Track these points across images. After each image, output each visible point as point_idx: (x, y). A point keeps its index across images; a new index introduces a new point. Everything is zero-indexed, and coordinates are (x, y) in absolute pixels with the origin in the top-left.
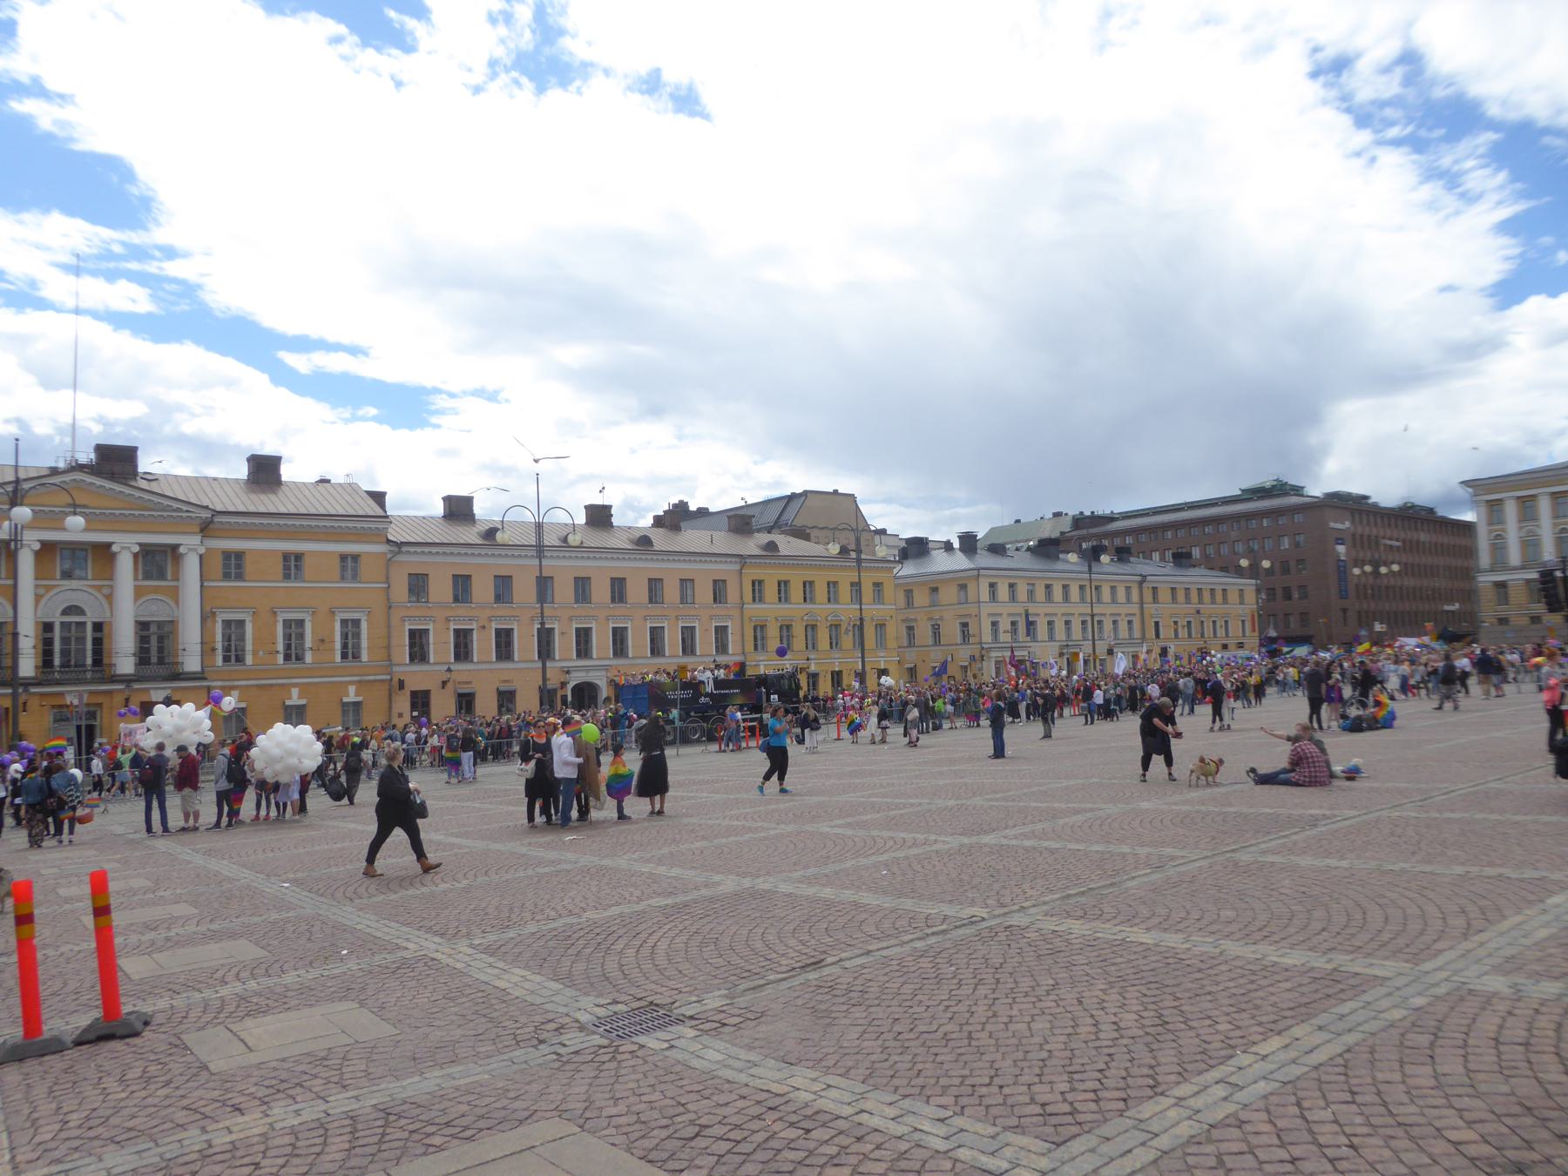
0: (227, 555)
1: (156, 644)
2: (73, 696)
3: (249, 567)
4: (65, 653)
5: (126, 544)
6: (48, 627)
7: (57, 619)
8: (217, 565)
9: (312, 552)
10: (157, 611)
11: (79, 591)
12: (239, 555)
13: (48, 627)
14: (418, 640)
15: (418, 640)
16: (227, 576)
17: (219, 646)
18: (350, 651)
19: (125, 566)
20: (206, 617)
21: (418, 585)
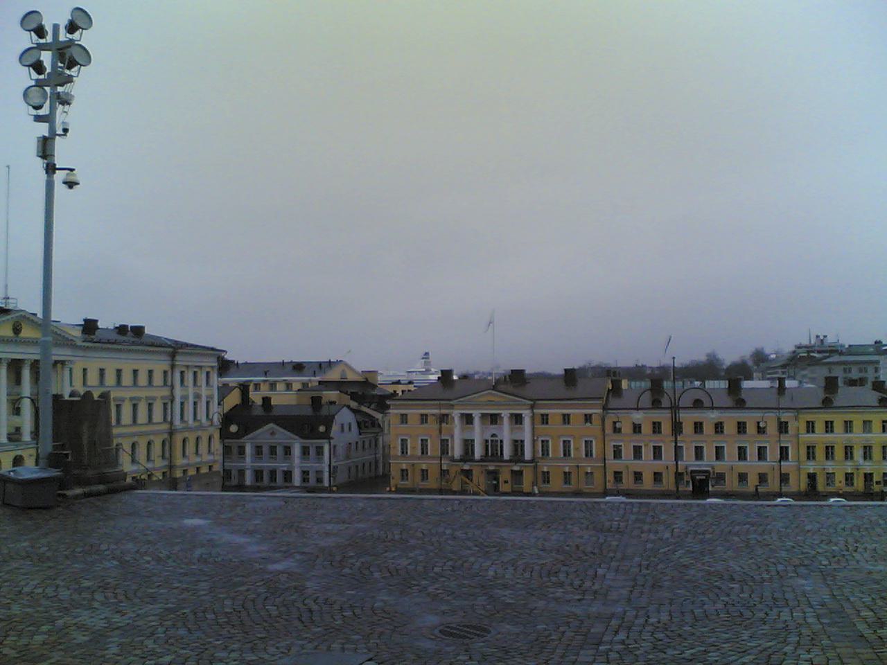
0: (542, 415)
1: (518, 445)
5: (505, 414)
6: (487, 441)
7: (490, 439)
8: (538, 419)
9: (573, 414)
10: (518, 437)
11: (493, 429)
18: (589, 453)
19: (506, 420)
20: (534, 442)
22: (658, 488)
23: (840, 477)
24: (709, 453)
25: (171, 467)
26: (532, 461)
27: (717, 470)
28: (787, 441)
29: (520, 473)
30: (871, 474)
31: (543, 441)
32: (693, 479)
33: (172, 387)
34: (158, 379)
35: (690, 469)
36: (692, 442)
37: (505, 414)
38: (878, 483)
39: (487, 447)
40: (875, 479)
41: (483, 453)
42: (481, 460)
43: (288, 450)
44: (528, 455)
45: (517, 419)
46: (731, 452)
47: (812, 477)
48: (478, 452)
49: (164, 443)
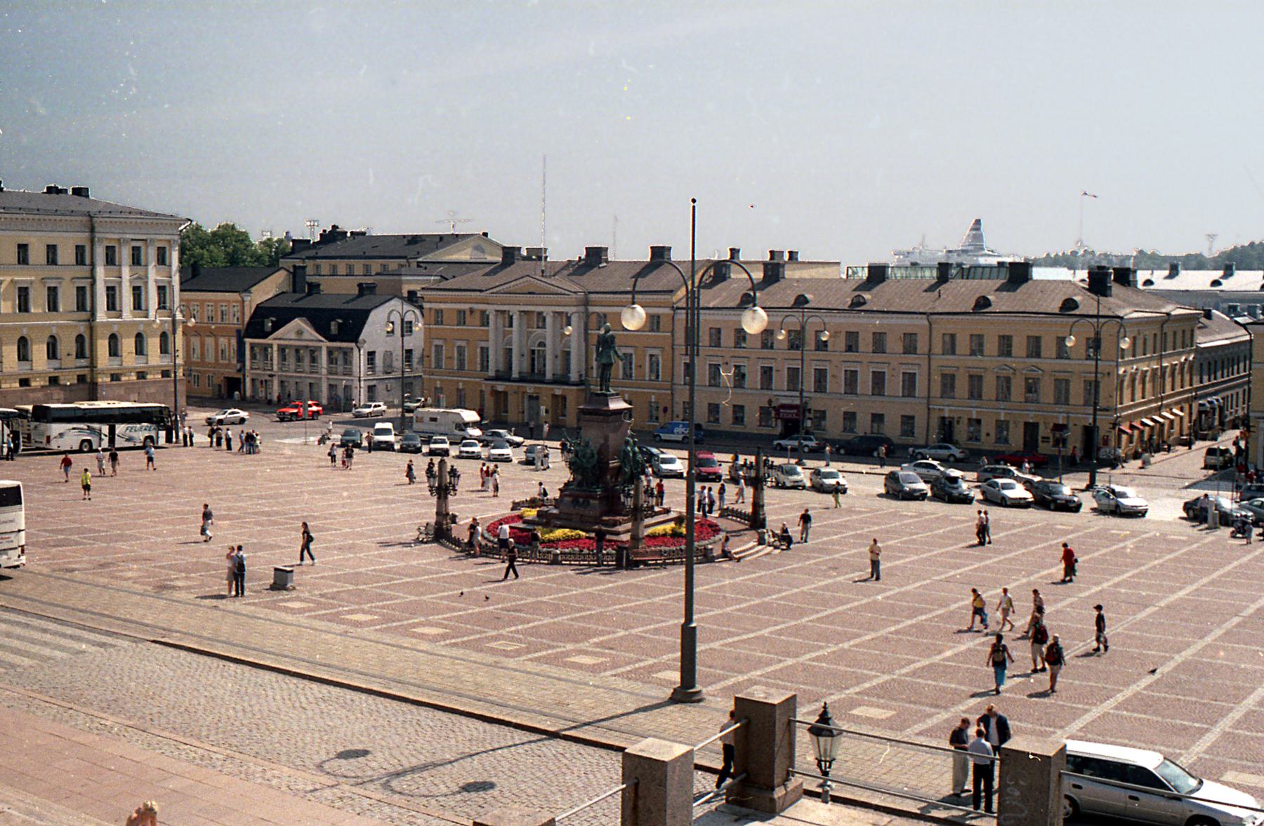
2: (530, 388)
5: (547, 311)
6: (533, 352)
19: (549, 320)
22: (738, 429)
23: (988, 427)
25: (92, 366)
26: (581, 383)
29: (564, 398)
33: (93, 265)
34: (66, 255)
38: (1045, 439)
39: (533, 359)
41: (526, 366)
42: (522, 379)
43: (313, 354)
49: (80, 339)
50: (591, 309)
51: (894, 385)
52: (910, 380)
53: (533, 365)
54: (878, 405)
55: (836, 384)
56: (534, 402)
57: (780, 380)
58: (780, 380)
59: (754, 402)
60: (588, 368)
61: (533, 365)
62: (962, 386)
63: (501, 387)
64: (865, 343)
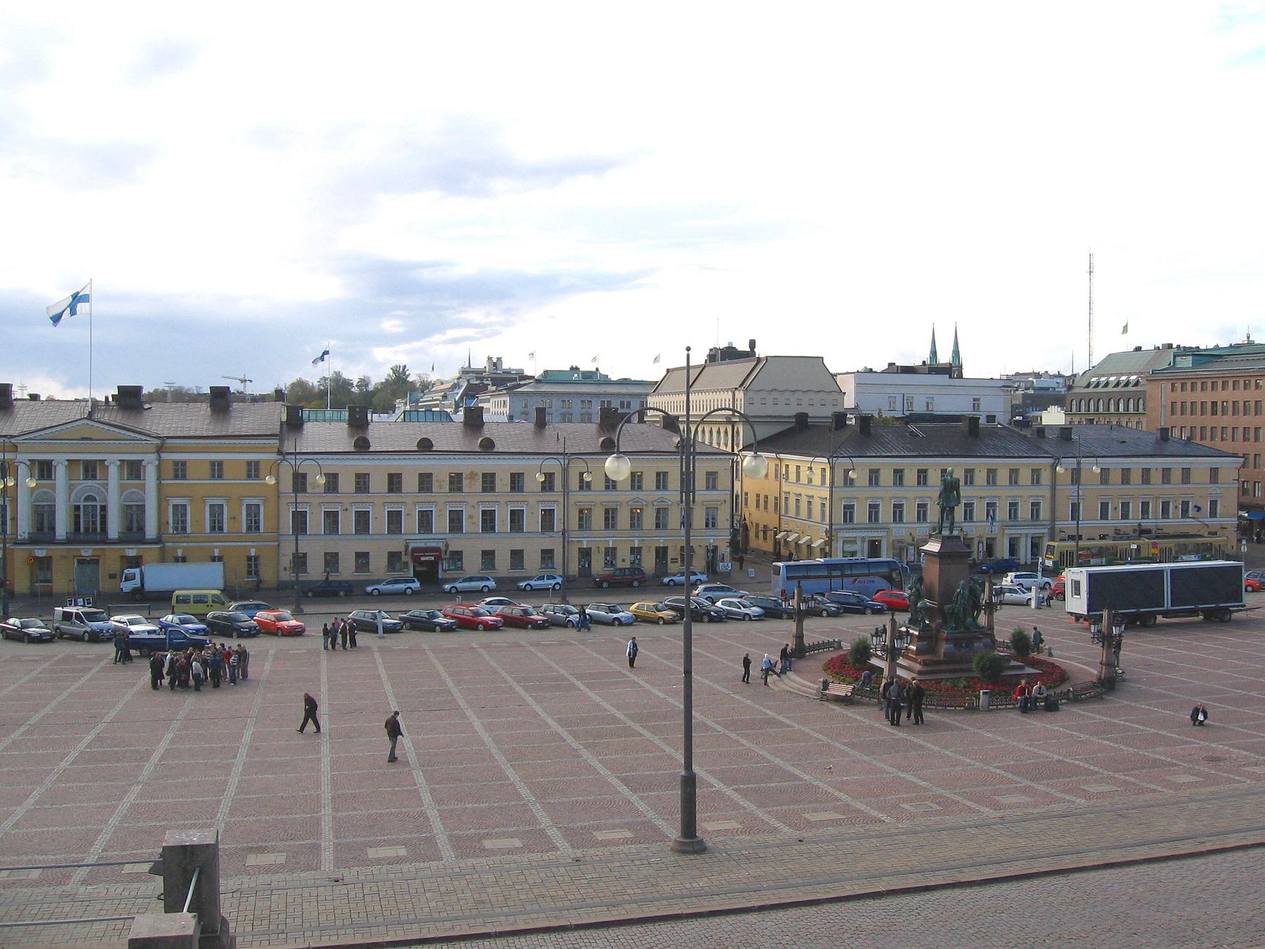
0: (176, 463)
1: (133, 517)
2: (87, 551)
3: (190, 471)
4: (87, 522)
5: (113, 459)
6: (77, 508)
7: (82, 504)
8: (170, 470)
12: (184, 463)
13: (77, 508)
14: (300, 521)
15: (300, 521)
16: (176, 477)
17: (171, 521)
18: (253, 525)
19: (113, 471)
21: (300, 482)
24: (441, 523)
26: (158, 541)
27: (454, 547)
28: (554, 500)
30: (665, 549)
31: (175, 507)
32: (416, 560)
35: (412, 545)
36: (415, 504)
37: (113, 459)
38: (674, 560)
39: (77, 517)
40: (671, 554)
42: (68, 541)
44: (151, 531)
45: (134, 469)
46: (472, 522)
47: (585, 554)
48: (62, 527)
50: (165, 456)
51: (532, 521)
52: (548, 515)
53: (77, 523)
54: (488, 542)
55: (472, 522)
56: (88, 569)
57: (410, 523)
58: (410, 523)
59: (379, 546)
60: (161, 524)
61: (77, 523)
62: (598, 518)
63: (41, 552)
64: (503, 482)
